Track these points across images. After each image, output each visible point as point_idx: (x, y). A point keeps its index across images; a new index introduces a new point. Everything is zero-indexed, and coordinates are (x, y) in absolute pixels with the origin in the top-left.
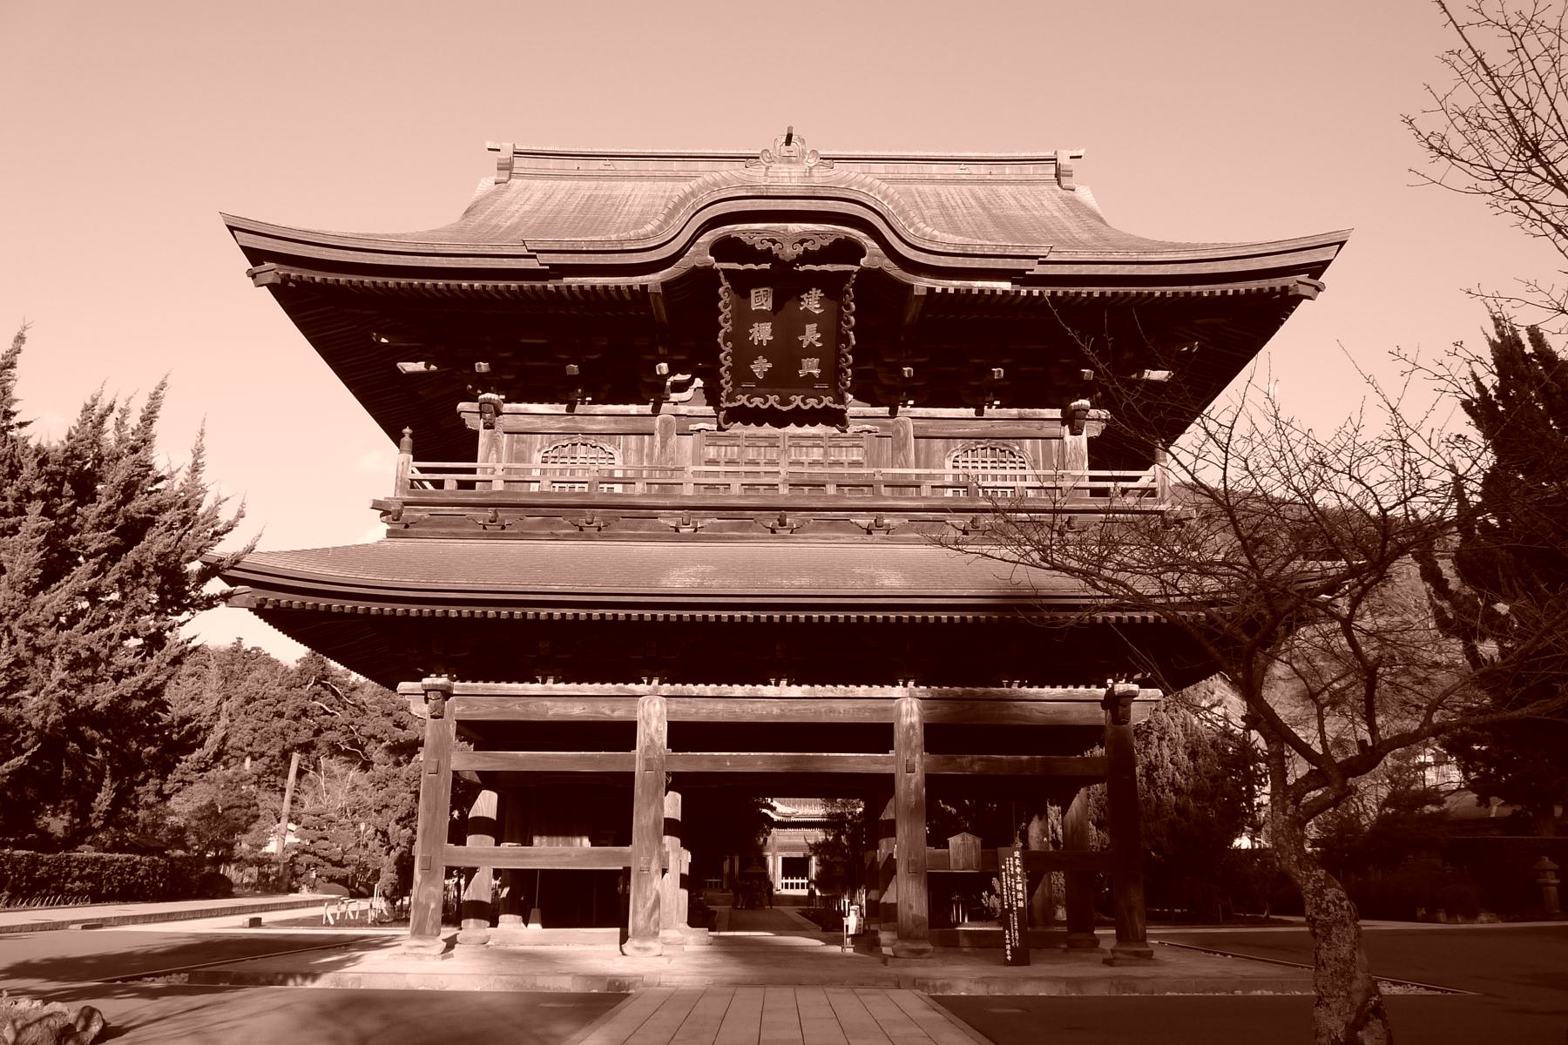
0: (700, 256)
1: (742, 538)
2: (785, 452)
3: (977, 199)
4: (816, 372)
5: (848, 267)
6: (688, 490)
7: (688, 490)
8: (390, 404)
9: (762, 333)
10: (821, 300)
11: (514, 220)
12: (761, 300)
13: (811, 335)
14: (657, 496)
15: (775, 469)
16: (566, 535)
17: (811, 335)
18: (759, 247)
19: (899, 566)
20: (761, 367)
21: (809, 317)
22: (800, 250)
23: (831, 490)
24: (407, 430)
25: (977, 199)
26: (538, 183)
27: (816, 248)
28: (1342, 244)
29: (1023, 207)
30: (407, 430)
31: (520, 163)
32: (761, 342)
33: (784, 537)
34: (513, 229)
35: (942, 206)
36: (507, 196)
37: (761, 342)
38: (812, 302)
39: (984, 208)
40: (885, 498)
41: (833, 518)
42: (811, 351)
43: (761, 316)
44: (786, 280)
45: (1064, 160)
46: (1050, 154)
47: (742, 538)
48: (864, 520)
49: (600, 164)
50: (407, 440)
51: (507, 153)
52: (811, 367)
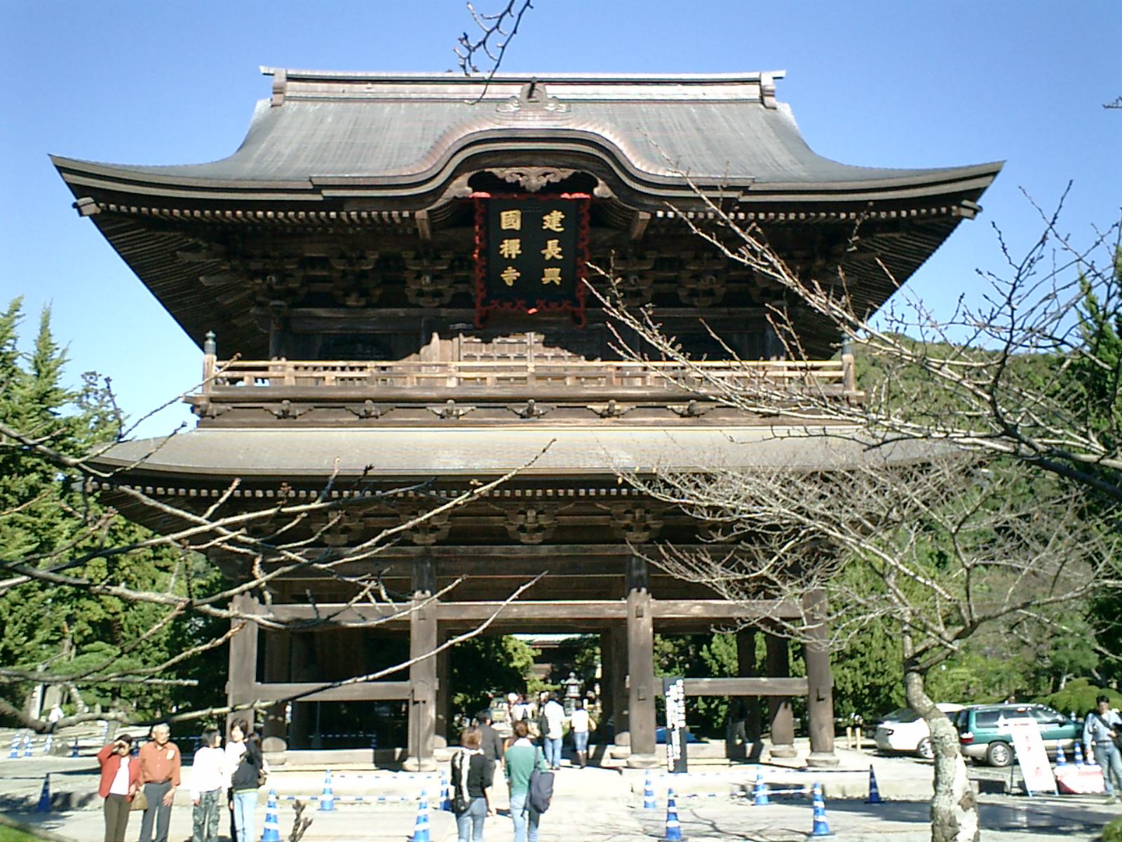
0: (461, 187)
1: (498, 422)
2: (531, 347)
3: (693, 121)
4: (557, 280)
5: (582, 196)
6: (452, 383)
7: (452, 383)
8: (195, 313)
9: (511, 248)
10: (562, 221)
11: (295, 146)
12: (511, 220)
13: (552, 249)
14: (424, 388)
15: (522, 363)
16: (349, 422)
17: (552, 249)
18: (509, 180)
19: (626, 447)
20: (510, 275)
21: (551, 234)
22: (544, 181)
23: (569, 381)
24: (210, 334)
25: (693, 121)
26: (309, 106)
27: (557, 180)
28: (995, 174)
29: (733, 130)
30: (210, 334)
31: (294, 88)
32: (510, 255)
33: (534, 422)
34: (295, 157)
35: (663, 129)
36: (285, 121)
37: (510, 255)
38: (553, 221)
39: (698, 129)
40: (616, 387)
41: (573, 405)
42: (553, 263)
43: (511, 234)
44: (534, 204)
45: (767, 81)
46: (755, 75)
47: (498, 422)
48: (599, 407)
49: (363, 87)
50: (210, 342)
51: (280, 79)
52: (552, 275)
